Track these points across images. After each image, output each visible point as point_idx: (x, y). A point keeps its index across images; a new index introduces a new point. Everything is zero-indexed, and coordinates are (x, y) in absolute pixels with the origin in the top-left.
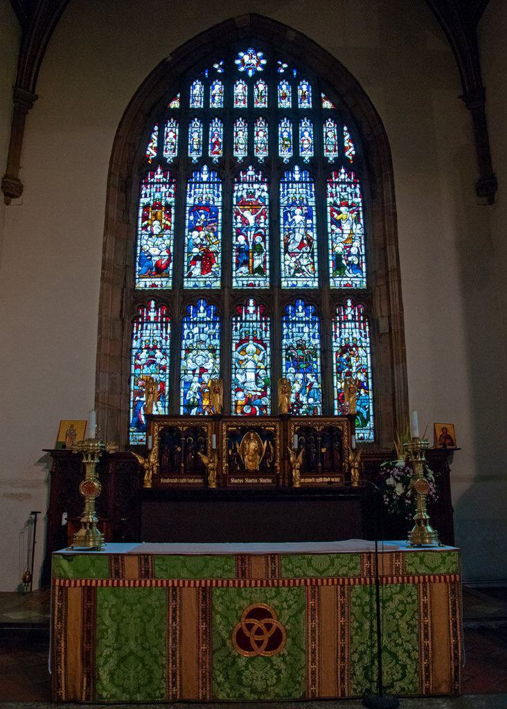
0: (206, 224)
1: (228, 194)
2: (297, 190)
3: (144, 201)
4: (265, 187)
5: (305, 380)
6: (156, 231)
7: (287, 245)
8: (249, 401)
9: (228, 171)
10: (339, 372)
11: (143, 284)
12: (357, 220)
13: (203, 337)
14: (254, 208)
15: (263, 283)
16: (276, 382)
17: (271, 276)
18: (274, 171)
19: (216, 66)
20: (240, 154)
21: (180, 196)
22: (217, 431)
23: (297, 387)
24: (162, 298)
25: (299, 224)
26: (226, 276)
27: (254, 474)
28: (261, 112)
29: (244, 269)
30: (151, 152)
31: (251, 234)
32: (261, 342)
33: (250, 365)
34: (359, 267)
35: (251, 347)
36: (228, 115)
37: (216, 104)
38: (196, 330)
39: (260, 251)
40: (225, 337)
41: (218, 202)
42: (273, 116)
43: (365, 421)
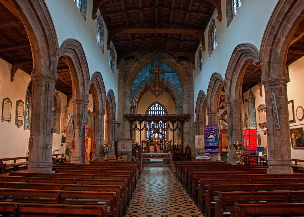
28: (157, 111)
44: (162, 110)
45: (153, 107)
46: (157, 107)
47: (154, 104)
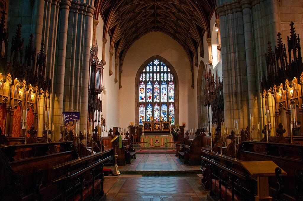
0: (150, 91)
1: (153, 87)
2: (164, 86)
3: (140, 88)
4: (159, 85)
5: (165, 116)
6: (142, 93)
7: (162, 95)
8: (156, 119)
9: (153, 83)
10: (170, 115)
11: (141, 101)
12: (173, 91)
13: (150, 109)
14: (157, 89)
15: (158, 101)
16: (160, 116)
17: (160, 100)
18: (160, 82)
19: (151, 63)
20: (155, 80)
21: (146, 87)
22: (152, 124)
23: (163, 117)
24: (144, 104)
25: (164, 92)
26: (153, 100)
27: (157, 129)
28: (158, 72)
29: (156, 99)
30: (141, 79)
31: (157, 93)
32: (158, 110)
33: (157, 114)
34: (173, 98)
35: (157, 111)
36: (153, 73)
37: (151, 71)
38: (148, 108)
39: (158, 96)
40: (153, 109)
41: (152, 88)
42: (160, 72)
43: (173, 122)
44: (165, 70)
45: (149, 67)
46: (157, 66)
47: (152, 59)
